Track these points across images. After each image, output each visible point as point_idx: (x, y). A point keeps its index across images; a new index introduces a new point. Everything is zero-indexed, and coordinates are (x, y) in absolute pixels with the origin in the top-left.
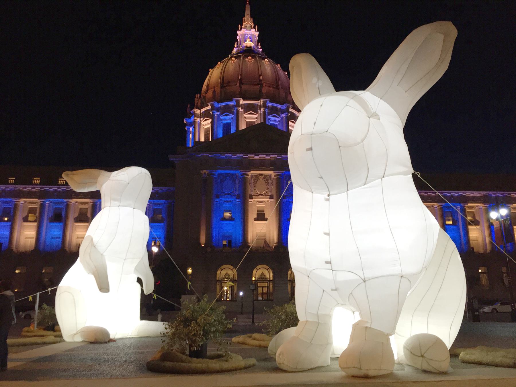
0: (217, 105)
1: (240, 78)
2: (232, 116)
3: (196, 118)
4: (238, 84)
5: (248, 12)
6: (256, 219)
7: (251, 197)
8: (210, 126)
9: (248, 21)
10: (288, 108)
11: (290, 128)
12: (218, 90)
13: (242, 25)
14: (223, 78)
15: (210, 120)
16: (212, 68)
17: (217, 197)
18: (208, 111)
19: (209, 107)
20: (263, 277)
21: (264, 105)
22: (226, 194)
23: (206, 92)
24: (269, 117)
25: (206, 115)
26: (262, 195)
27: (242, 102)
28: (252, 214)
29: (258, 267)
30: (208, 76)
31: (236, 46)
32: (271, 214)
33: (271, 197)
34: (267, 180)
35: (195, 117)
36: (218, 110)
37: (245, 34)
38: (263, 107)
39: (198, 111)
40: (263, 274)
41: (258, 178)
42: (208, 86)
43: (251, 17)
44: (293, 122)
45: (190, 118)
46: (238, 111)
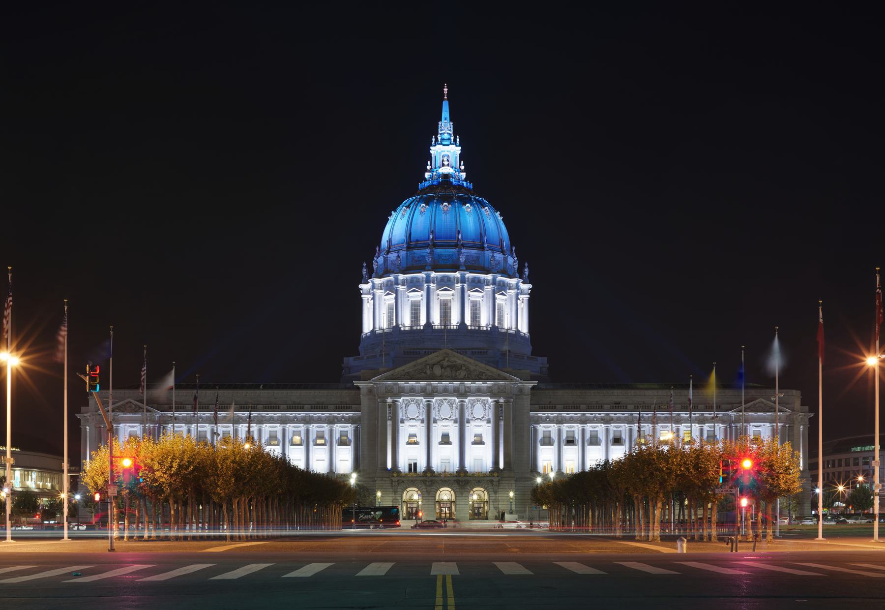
0: (401, 277)
2: (422, 292)
4: (429, 251)
5: (445, 113)
6: (440, 443)
7: (435, 422)
8: (393, 301)
9: (446, 127)
11: (497, 302)
12: (403, 253)
13: (436, 134)
14: (410, 234)
15: (394, 295)
16: (395, 211)
17: (402, 422)
18: (390, 281)
21: (463, 280)
24: (469, 292)
25: (390, 288)
27: (433, 274)
28: (436, 438)
29: (441, 489)
30: (391, 219)
31: (429, 167)
32: (454, 438)
33: (455, 422)
34: (452, 404)
37: (440, 153)
39: (378, 281)
42: (390, 241)
43: (451, 120)
44: (502, 294)
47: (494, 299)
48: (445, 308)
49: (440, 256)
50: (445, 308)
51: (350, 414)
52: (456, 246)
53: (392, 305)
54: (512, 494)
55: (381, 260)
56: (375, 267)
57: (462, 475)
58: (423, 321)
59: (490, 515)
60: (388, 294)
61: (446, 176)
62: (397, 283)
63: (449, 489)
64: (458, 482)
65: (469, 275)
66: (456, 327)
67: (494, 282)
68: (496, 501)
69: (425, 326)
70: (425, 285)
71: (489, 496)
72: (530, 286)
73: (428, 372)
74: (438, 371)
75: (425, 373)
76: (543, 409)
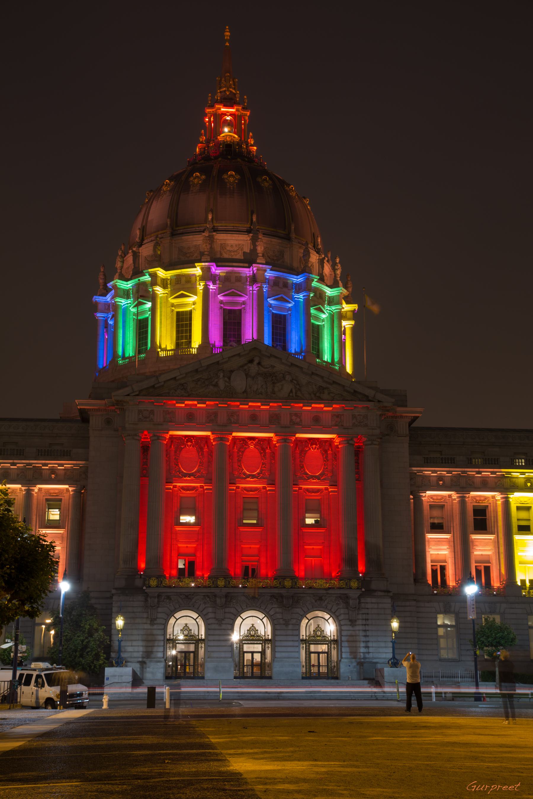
0: (161, 273)
1: (210, 217)
2: (193, 298)
3: (118, 299)
8: (148, 315)
10: (309, 281)
15: (149, 305)
19: (147, 278)
20: (252, 633)
22: (186, 475)
23: (141, 245)
26: (253, 477)
29: (244, 615)
36: (164, 284)
40: (253, 628)
41: (246, 444)
42: (143, 229)
47: (308, 315)
49: (223, 246)
51: (68, 464)
52: (249, 231)
53: (147, 319)
54: (395, 625)
55: (130, 259)
56: (119, 264)
57: (288, 583)
58: (197, 340)
59: (344, 669)
61: (229, 146)
62: (154, 283)
63: (261, 615)
64: (278, 599)
65: (269, 274)
67: (306, 287)
68: (353, 641)
69: (200, 348)
70: (200, 287)
71: (340, 631)
72: (354, 307)
73: (222, 384)
74: (239, 382)
75: (216, 385)
76: (429, 462)
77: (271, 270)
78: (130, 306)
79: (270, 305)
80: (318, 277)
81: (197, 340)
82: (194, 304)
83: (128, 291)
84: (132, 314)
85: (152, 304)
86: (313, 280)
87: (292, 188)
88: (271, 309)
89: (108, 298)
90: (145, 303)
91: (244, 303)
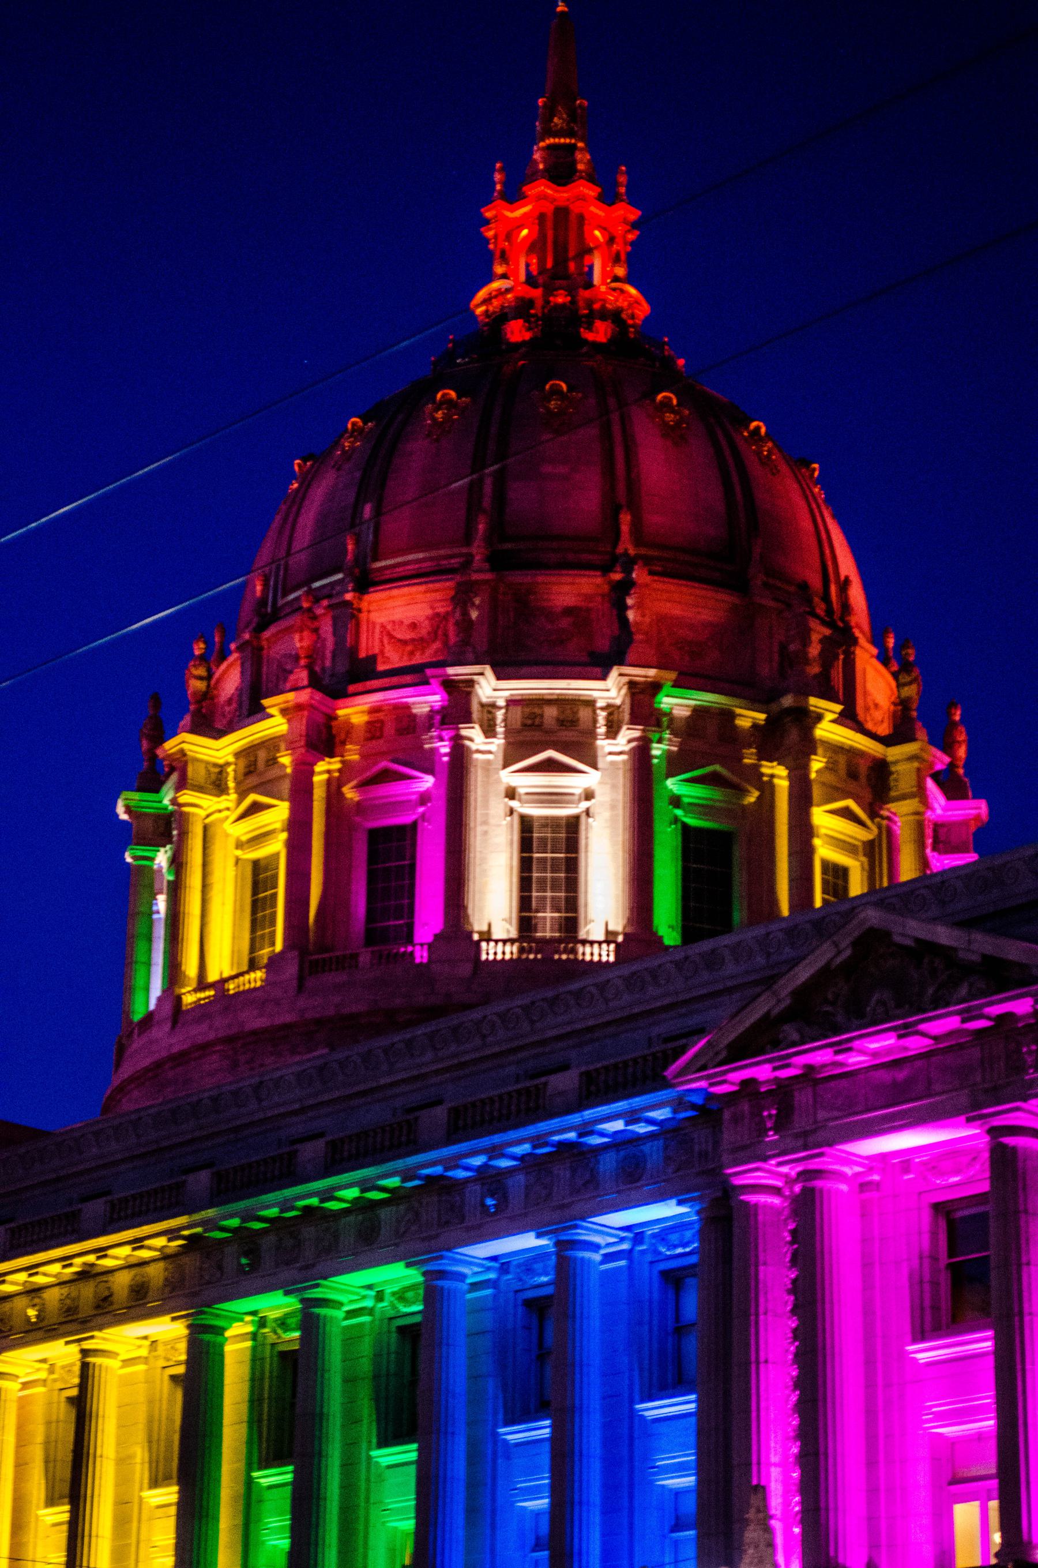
3: (187, 797)
8: (277, 846)
27: (490, 688)
35: (182, 785)
38: (634, 720)
45: (154, 786)
46: (460, 753)
48: (550, 853)
50: (550, 853)
60: (256, 808)
66: (607, 954)
77: (676, 685)
78: (227, 818)
79: (676, 801)
80: (838, 708)
81: (428, 922)
82: (424, 798)
83: (222, 768)
84: (231, 843)
85: (293, 811)
86: (819, 718)
87: (758, 428)
88: (679, 812)
89: (166, 797)
90: (270, 806)
91: (589, 795)
